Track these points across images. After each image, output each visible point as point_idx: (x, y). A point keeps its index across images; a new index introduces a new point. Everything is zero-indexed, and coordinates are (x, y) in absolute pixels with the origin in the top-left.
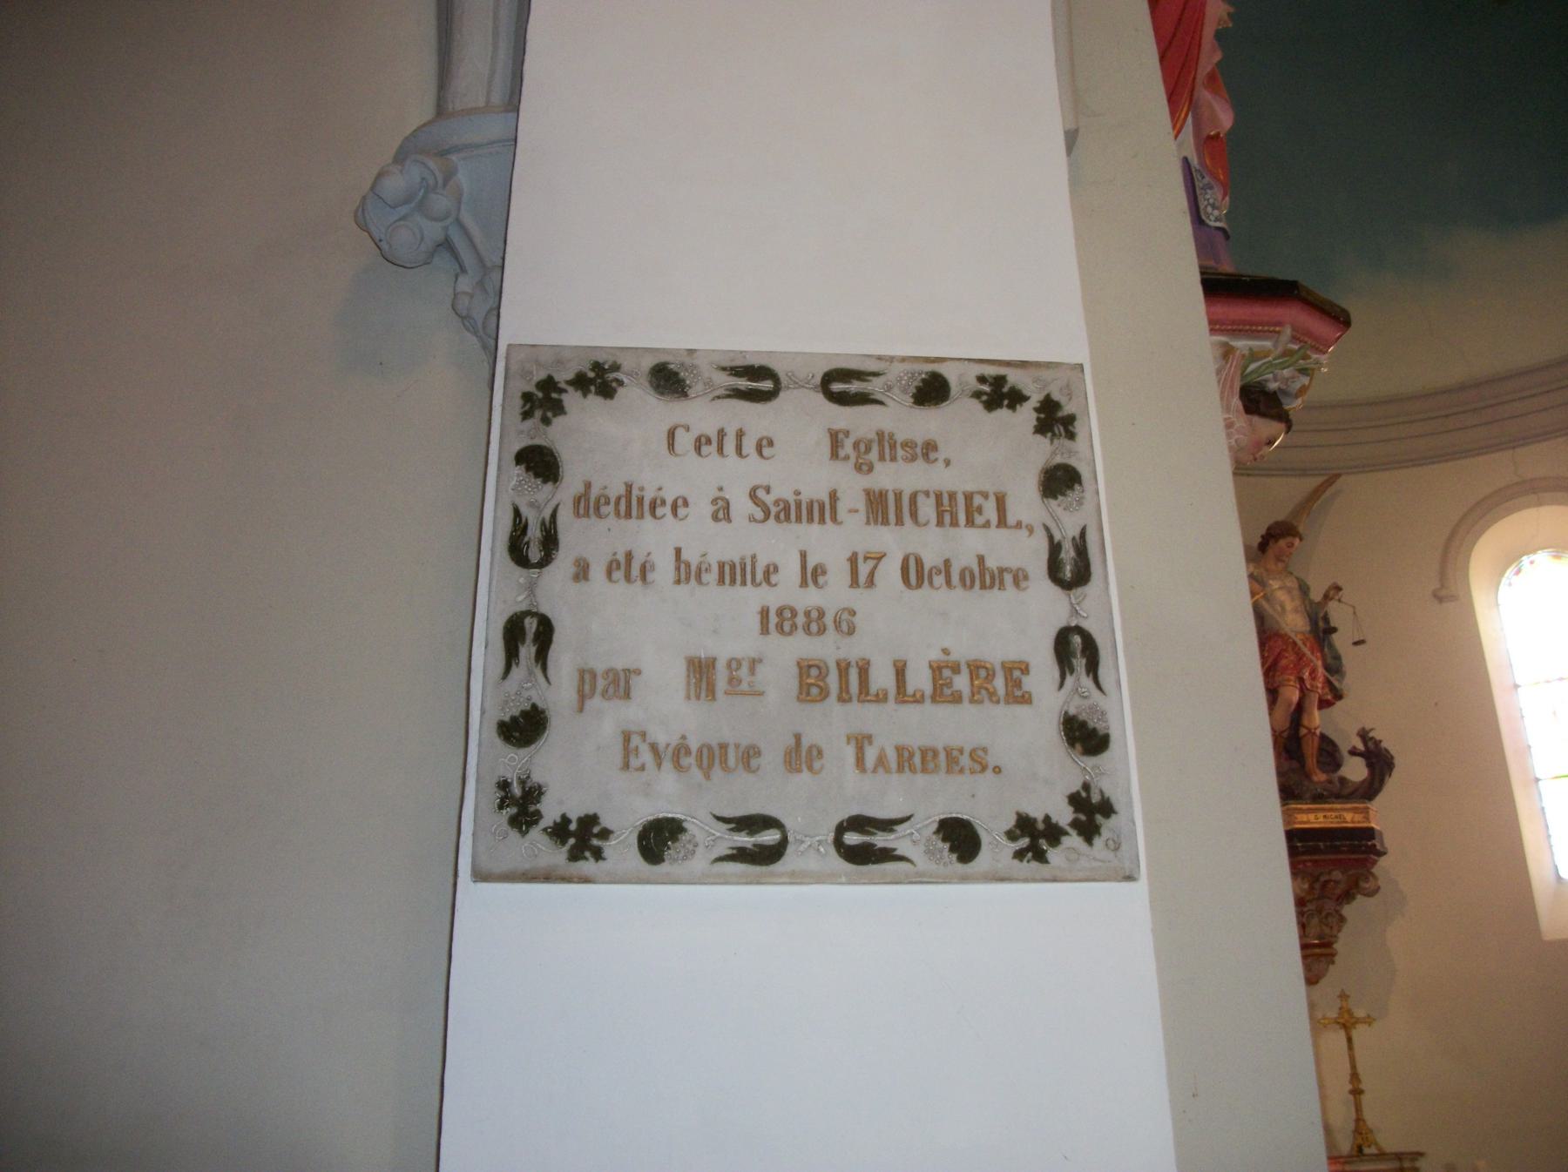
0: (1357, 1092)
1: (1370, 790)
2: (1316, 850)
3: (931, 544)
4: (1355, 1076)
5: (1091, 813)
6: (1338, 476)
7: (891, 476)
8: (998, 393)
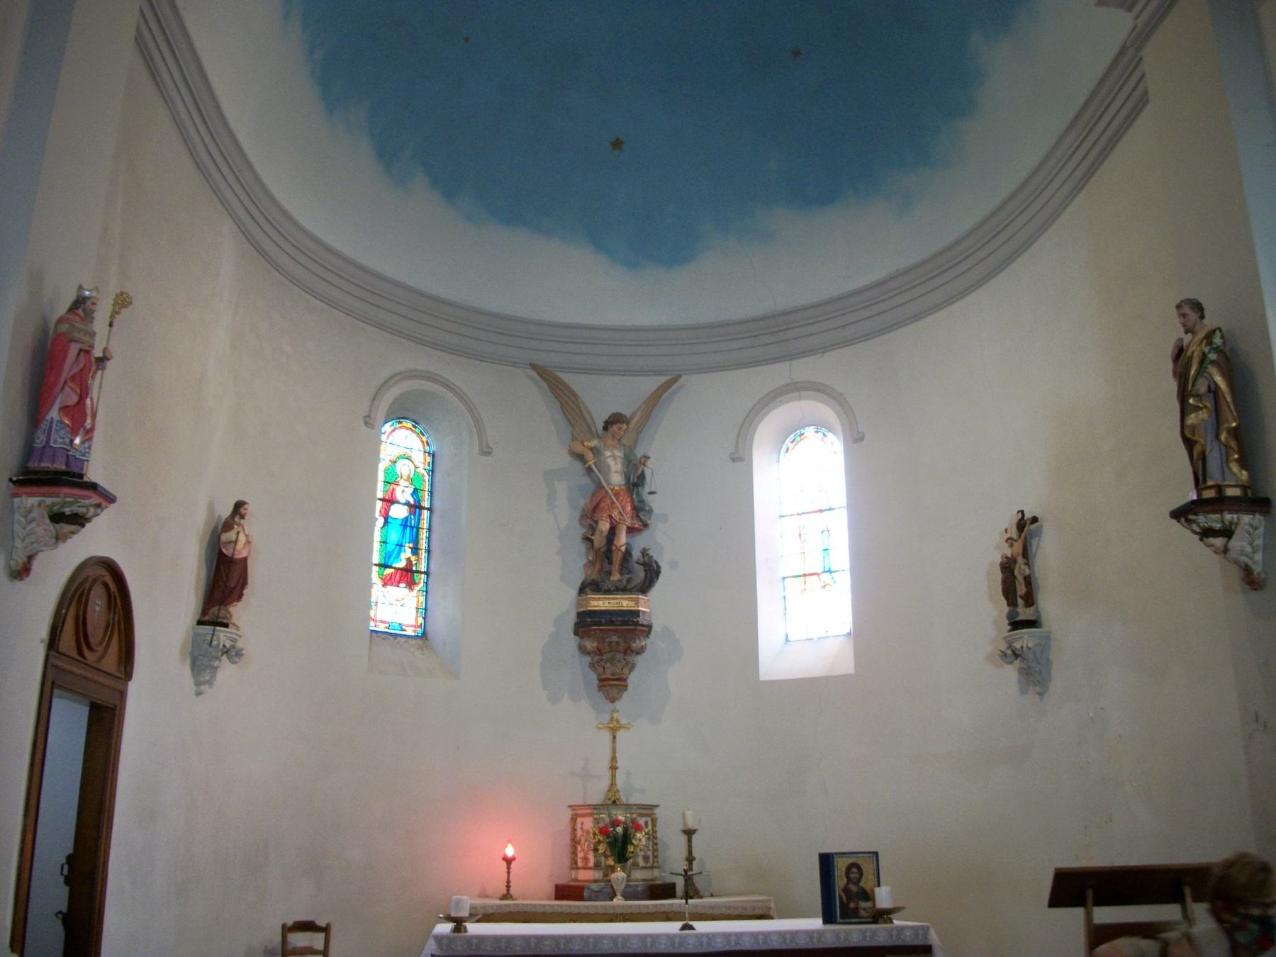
0: (614, 768)
1: (645, 588)
2: (599, 624)
4: (614, 759)
6: (680, 376)
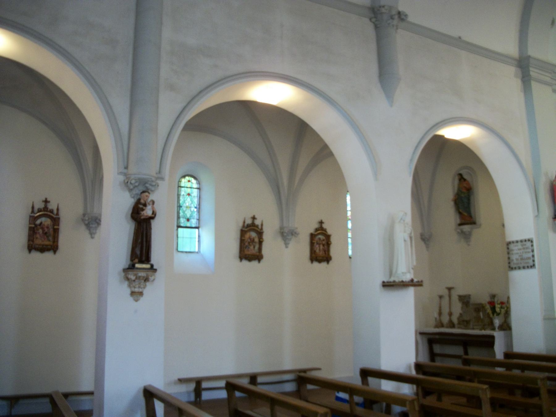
3: (526, 250)
5: (534, 265)
7: (524, 247)
8: (529, 240)
